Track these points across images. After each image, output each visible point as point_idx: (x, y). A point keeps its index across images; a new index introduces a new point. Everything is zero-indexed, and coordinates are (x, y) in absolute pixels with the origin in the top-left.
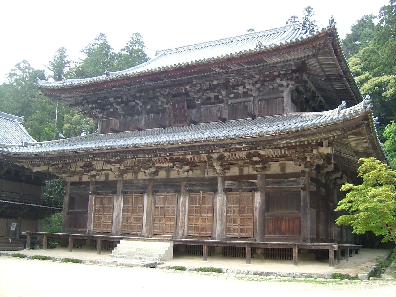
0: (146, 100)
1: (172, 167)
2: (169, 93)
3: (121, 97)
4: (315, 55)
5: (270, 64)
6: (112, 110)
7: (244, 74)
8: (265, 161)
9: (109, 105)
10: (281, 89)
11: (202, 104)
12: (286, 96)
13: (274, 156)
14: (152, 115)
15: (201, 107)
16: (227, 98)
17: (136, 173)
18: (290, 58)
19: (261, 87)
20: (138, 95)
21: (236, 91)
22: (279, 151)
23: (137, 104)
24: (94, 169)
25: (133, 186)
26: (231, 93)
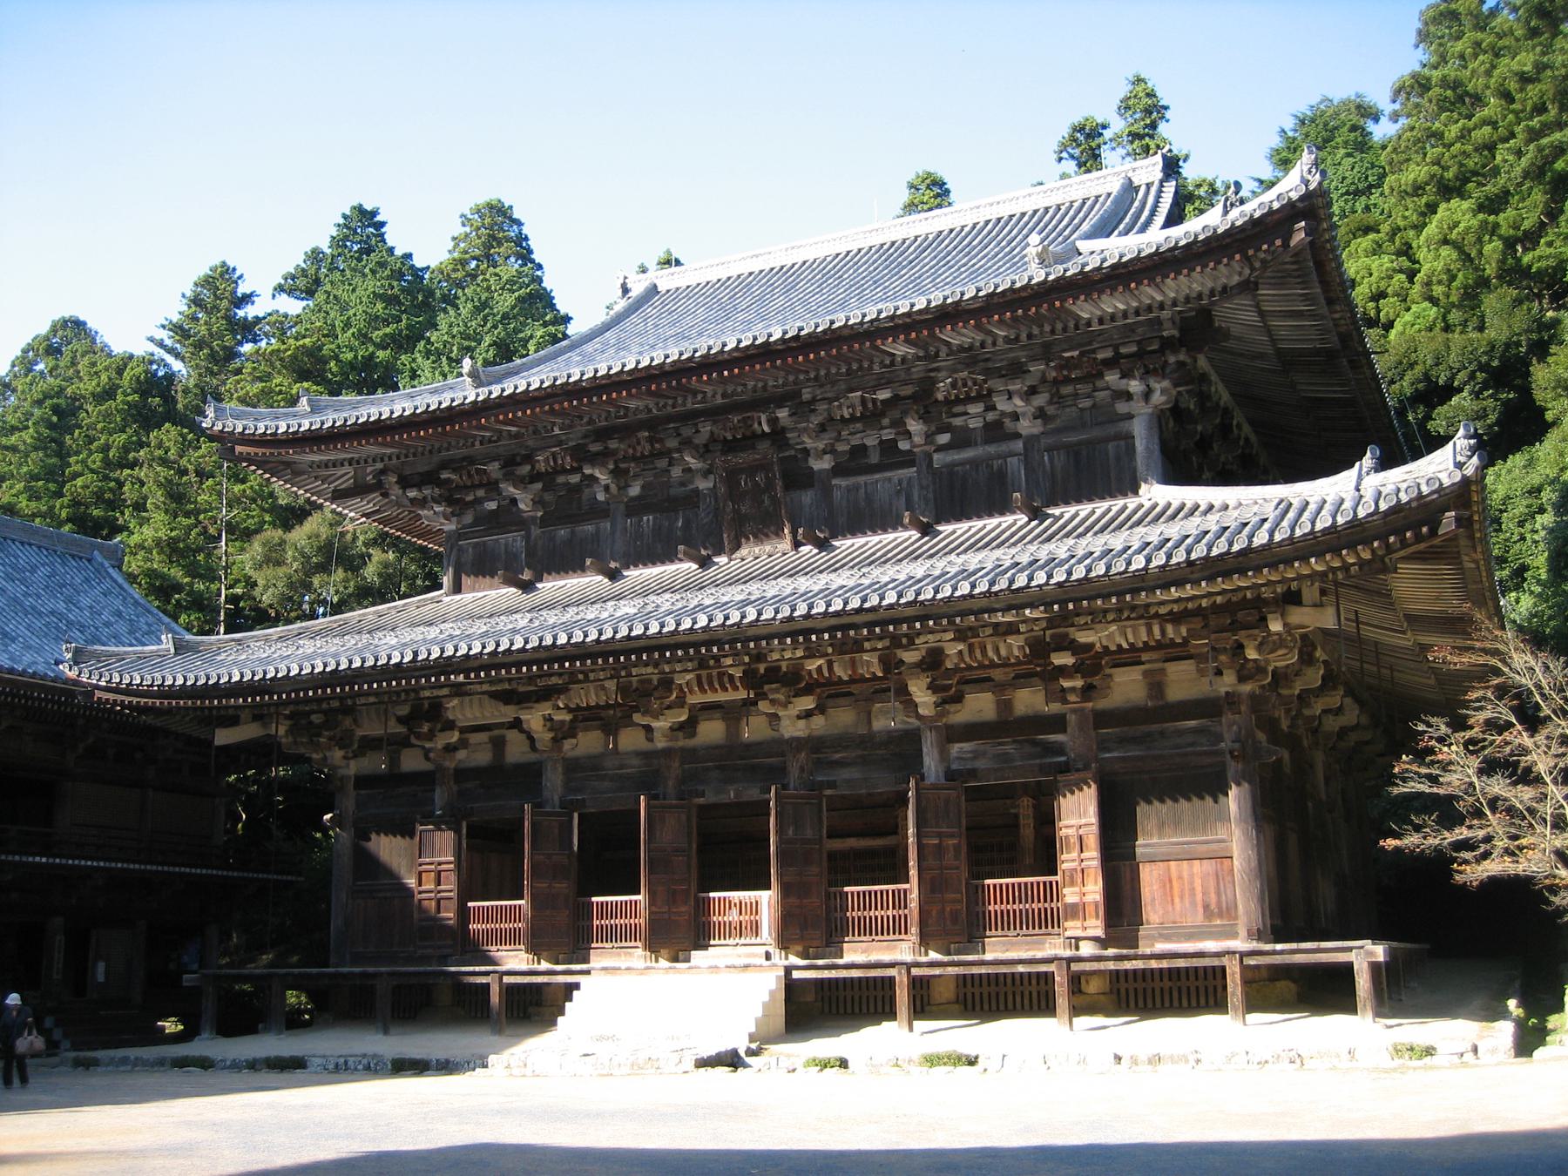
0: (622, 466)
1: (749, 704)
2: (713, 438)
3: (529, 458)
4: (1248, 287)
5: (1089, 324)
6: (492, 505)
7: (987, 360)
8: (1093, 664)
9: (481, 486)
10: (1122, 407)
11: (838, 471)
12: (1140, 430)
13: (1125, 646)
14: (648, 519)
16: (927, 448)
18: (1159, 298)
19: (1050, 402)
20: (595, 448)
21: (957, 422)
22: (1143, 630)
23: (593, 479)
24: (450, 726)
26: (941, 431)
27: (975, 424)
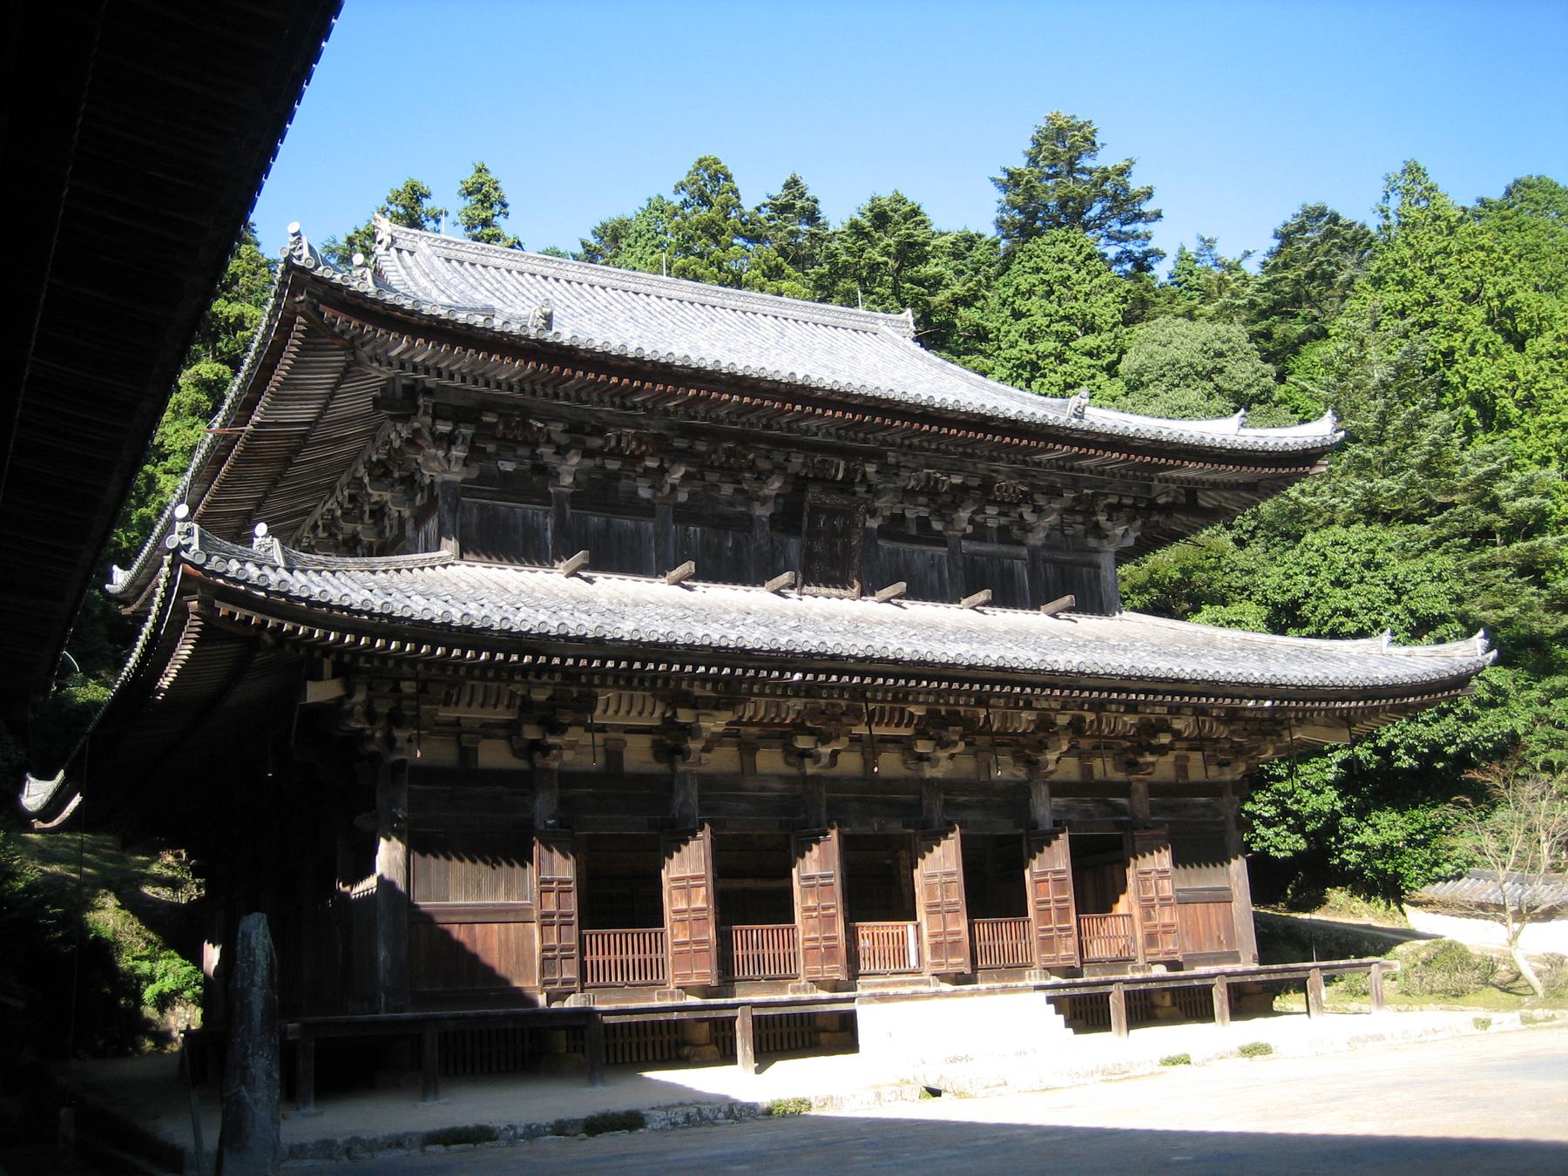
6: (509, 467)
11: (883, 532)
15: (880, 542)
17: (748, 749)
20: (681, 443)
25: (742, 798)
27: (992, 523)
